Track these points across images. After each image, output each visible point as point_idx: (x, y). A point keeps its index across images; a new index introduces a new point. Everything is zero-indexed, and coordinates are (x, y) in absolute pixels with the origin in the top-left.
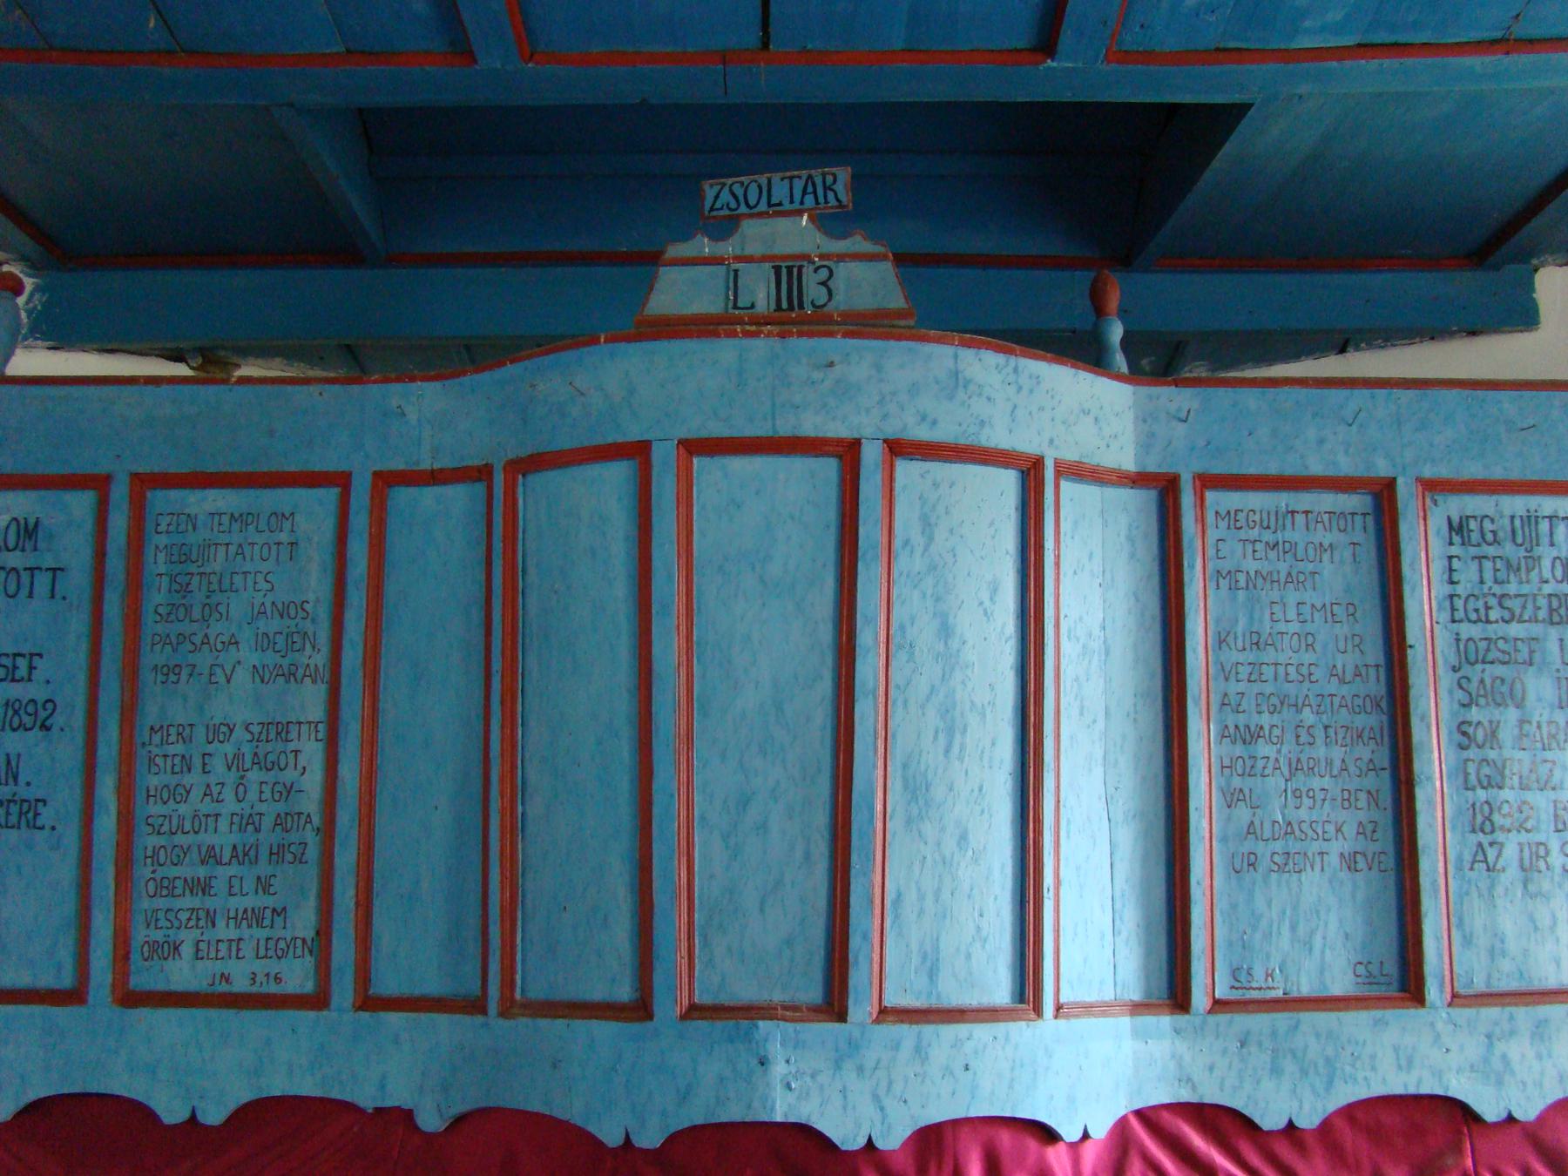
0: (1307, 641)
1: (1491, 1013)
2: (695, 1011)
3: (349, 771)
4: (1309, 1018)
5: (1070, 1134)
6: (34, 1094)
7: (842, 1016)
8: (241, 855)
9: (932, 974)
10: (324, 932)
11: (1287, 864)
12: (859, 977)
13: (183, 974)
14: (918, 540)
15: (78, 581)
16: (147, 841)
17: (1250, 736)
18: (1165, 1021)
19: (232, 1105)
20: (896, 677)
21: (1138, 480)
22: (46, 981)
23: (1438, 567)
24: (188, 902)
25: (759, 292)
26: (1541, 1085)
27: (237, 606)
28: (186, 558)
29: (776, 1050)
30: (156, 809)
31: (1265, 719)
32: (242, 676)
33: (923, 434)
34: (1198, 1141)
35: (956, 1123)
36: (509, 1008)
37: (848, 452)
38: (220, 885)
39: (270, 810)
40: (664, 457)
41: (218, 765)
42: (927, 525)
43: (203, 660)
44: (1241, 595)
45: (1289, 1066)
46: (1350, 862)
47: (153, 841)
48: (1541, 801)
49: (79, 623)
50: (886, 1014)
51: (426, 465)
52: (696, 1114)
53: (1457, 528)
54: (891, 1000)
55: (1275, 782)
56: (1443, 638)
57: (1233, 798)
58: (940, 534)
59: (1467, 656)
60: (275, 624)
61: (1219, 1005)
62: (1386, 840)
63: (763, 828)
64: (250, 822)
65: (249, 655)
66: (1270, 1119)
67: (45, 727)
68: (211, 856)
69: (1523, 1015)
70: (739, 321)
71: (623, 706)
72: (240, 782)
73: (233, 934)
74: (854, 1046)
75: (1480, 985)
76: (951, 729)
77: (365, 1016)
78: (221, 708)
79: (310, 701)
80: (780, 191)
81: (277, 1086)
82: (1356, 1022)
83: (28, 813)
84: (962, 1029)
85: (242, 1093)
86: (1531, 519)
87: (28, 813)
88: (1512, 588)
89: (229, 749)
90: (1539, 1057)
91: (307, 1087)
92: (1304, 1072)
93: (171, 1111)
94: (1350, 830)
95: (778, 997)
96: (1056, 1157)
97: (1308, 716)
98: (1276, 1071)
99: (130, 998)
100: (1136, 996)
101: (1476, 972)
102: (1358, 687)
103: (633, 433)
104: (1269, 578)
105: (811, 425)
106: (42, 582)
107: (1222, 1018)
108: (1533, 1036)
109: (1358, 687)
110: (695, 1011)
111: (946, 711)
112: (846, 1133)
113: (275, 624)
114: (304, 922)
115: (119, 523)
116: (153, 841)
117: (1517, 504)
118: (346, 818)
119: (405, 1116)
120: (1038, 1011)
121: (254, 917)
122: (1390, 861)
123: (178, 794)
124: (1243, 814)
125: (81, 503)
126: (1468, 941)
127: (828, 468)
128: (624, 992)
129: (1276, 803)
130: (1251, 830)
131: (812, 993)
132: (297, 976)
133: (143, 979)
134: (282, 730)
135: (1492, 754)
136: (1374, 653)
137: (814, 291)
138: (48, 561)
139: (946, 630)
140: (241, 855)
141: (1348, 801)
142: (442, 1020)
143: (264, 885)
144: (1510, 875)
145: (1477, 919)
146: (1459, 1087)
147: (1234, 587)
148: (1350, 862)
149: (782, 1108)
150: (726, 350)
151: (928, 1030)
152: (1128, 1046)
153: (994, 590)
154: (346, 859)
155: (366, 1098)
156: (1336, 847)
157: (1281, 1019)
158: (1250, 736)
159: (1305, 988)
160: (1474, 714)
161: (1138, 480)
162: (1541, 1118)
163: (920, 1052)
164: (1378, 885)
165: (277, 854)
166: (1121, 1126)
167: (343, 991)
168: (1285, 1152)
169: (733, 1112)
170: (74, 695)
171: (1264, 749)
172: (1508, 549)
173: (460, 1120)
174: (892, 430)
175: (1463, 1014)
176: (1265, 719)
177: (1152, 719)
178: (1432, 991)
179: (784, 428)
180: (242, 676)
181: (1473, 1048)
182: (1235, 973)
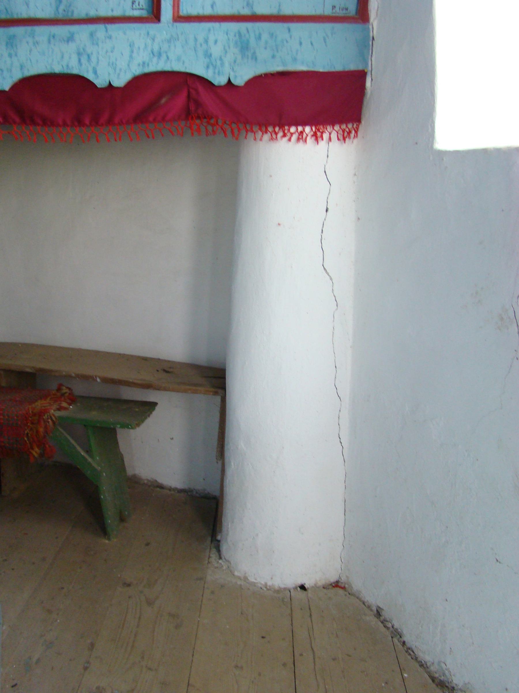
26: (11, 71)
90: (10, 56)
108: (7, 44)
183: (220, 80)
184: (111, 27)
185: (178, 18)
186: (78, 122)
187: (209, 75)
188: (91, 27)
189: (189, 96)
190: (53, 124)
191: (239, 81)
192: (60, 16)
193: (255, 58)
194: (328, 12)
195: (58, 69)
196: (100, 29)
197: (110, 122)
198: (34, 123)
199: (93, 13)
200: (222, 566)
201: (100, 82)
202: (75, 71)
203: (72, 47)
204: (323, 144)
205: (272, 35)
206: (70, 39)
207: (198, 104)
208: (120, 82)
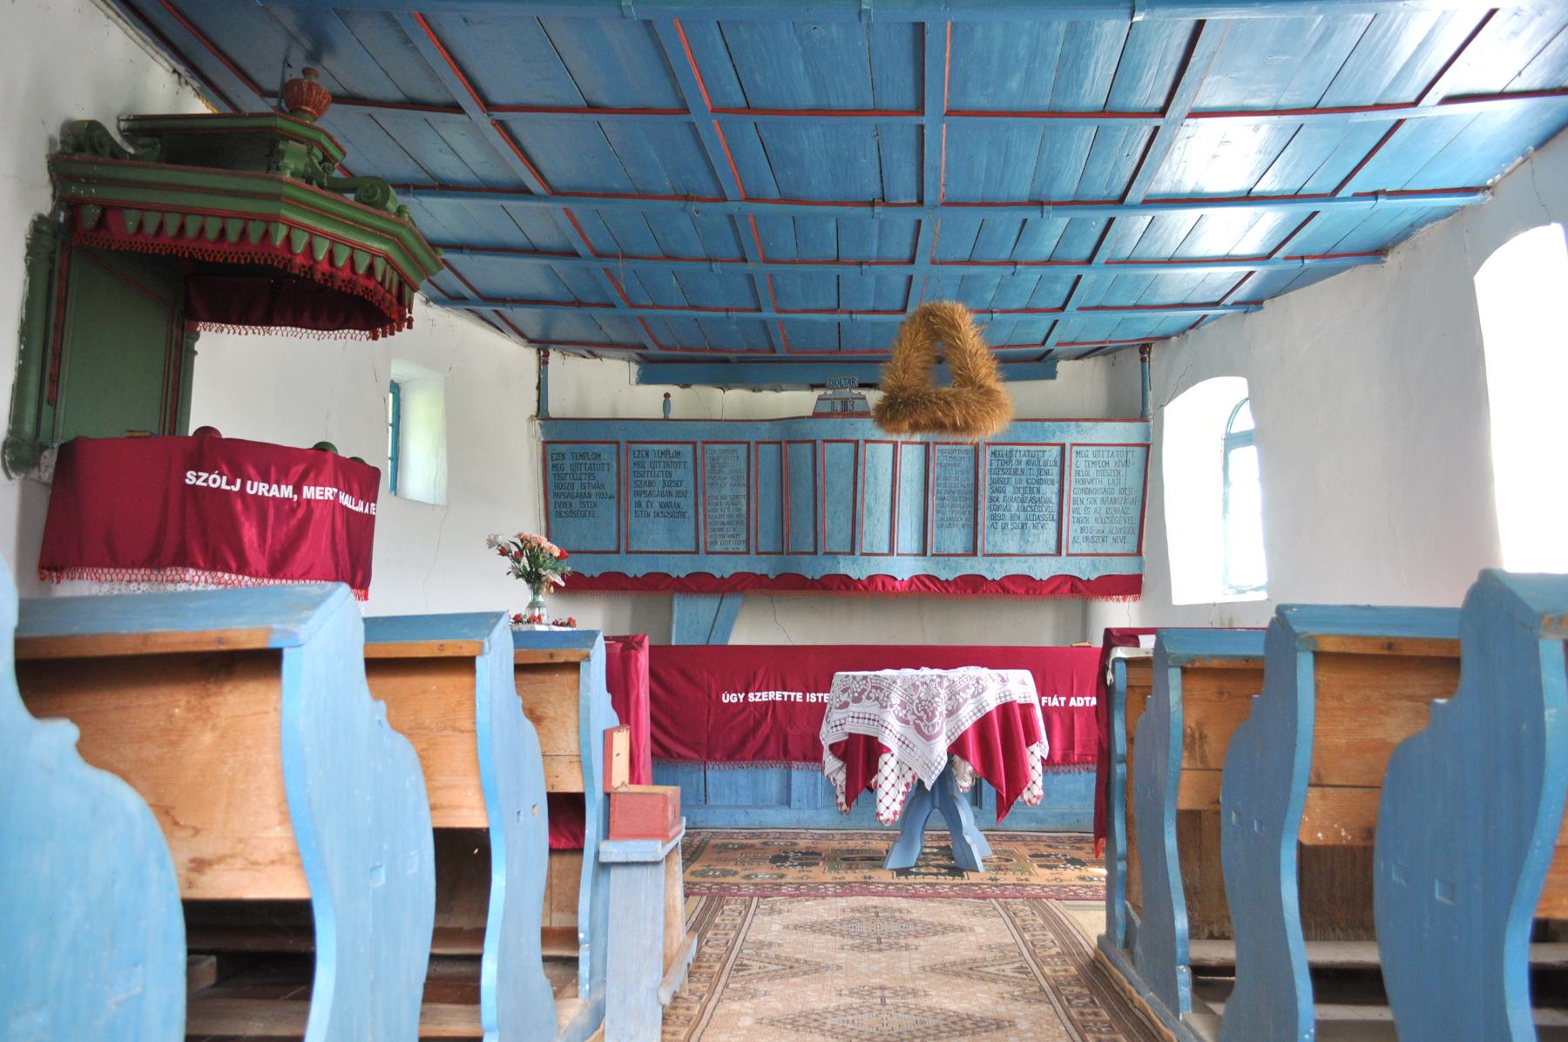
0: (957, 478)
1: (992, 558)
2: (826, 553)
3: (752, 506)
4: (952, 558)
5: (900, 579)
6: (690, 572)
7: (854, 554)
8: (729, 523)
9: (872, 547)
10: (748, 539)
11: (949, 526)
12: (857, 547)
13: (718, 548)
14: (870, 459)
15: (690, 464)
16: (709, 520)
17: (943, 499)
18: (921, 558)
19: (730, 574)
20: (865, 488)
21: (921, 443)
22: (689, 550)
23: (988, 463)
24: (718, 533)
25: (838, 407)
27: (726, 470)
28: (714, 459)
29: (841, 560)
30: (710, 513)
31: (946, 496)
32: (728, 485)
33: (872, 438)
34: (927, 582)
35: (876, 575)
36: (788, 554)
37: (857, 442)
38: (725, 530)
39: (735, 514)
40: (818, 443)
41: (724, 505)
42: (873, 457)
43: (719, 482)
44: (943, 468)
45: (947, 568)
46: (963, 526)
47: (710, 520)
48: (1007, 514)
49: (691, 474)
50: (862, 554)
51: (767, 440)
52: (826, 572)
53: (994, 453)
54: (864, 551)
55: (948, 509)
56: (987, 478)
57: (938, 513)
58: (875, 458)
59: (993, 482)
60: (734, 474)
61: (933, 555)
62: (971, 522)
63: (839, 518)
64: (731, 516)
65: (728, 481)
66: (943, 578)
67: (685, 496)
68: (723, 523)
69: (998, 558)
70: (834, 414)
71: (811, 493)
72: (729, 509)
73: (728, 539)
74: (856, 560)
75: (991, 552)
76: (876, 498)
77: (757, 556)
78: (723, 493)
79: (743, 491)
80: (843, 383)
81: (740, 570)
82: (962, 559)
83: (683, 515)
84: (877, 557)
85: (733, 572)
86: (1011, 451)
87: (683, 515)
88: (1005, 467)
89: (726, 501)
91: (746, 571)
92: (950, 569)
93: (718, 575)
94: (964, 519)
95: (842, 551)
96: (897, 584)
97: (956, 495)
98: (944, 569)
99: (708, 553)
100: (915, 552)
101: (989, 549)
102: (968, 489)
103: (812, 438)
104: (949, 465)
105: (848, 438)
106: (682, 464)
107: (934, 558)
109: (968, 489)
110: (826, 553)
111: (875, 495)
112: (854, 576)
113: (734, 474)
114: (743, 536)
115: (699, 452)
116: (710, 520)
117: (1009, 448)
118: (752, 516)
119: (766, 576)
120: (893, 554)
121: (733, 536)
122: (972, 526)
123: (714, 510)
124: (940, 515)
125: (690, 447)
126: (989, 543)
127: (852, 445)
128: (812, 550)
129: (948, 513)
130: (942, 519)
131: (848, 550)
132: (742, 548)
133: (709, 549)
134: (737, 497)
135: (997, 504)
136: (972, 481)
137: (850, 407)
138: (683, 460)
139: (876, 479)
140: (729, 523)
141: (964, 513)
142: (774, 556)
143: (735, 529)
144: (1000, 529)
145: (991, 538)
146: (983, 573)
147: (941, 467)
148: (963, 526)
149: (842, 572)
150: (831, 421)
151: (871, 557)
152: (913, 562)
153: (886, 469)
154: (752, 524)
155: (758, 572)
156: (960, 523)
157: (946, 558)
158: (943, 499)
159: (953, 552)
160: (994, 495)
161: (921, 443)
162: (1001, 580)
163: (869, 562)
164: (968, 531)
165: (737, 523)
166: (911, 578)
167: (753, 551)
168: (945, 584)
169: (833, 572)
170: (691, 489)
171: (946, 502)
172: (1005, 458)
173: (778, 576)
174: (865, 438)
175: (985, 558)
176: (946, 496)
177: (921, 495)
178: (979, 554)
179: (843, 438)
180: (728, 485)
181: (987, 565)
182: (937, 549)
183: (1085, 578)
184: (1042, 558)
185: (1068, 555)
186: (1027, 592)
187: (1080, 576)
188: (1035, 557)
189: (1072, 585)
190: (1014, 592)
191: (1092, 579)
192: (1021, 552)
193: (1098, 569)
194: (1126, 552)
195: (1020, 573)
196: (1038, 558)
197: (1040, 593)
198: (1008, 592)
199: (1034, 552)
200: (1072, 847)
201: (1037, 578)
202: (1027, 574)
203: (1026, 565)
204: (1127, 603)
205: (1105, 561)
206: (1026, 562)
207: (1076, 588)
208: (1045, 578)
